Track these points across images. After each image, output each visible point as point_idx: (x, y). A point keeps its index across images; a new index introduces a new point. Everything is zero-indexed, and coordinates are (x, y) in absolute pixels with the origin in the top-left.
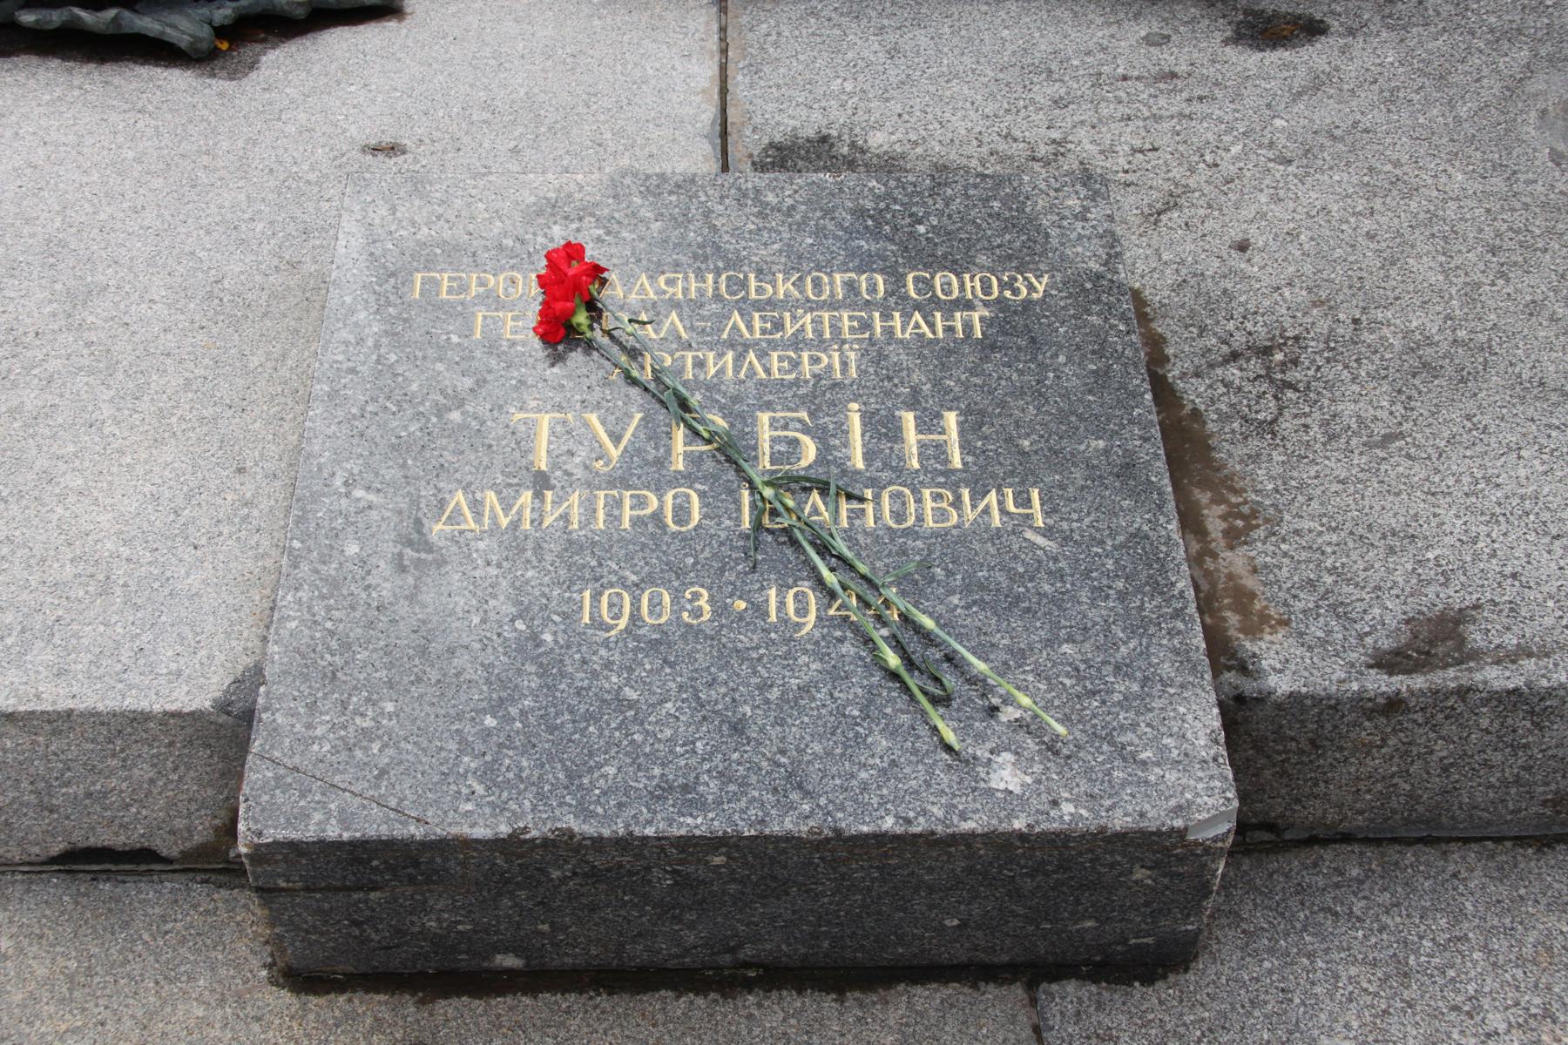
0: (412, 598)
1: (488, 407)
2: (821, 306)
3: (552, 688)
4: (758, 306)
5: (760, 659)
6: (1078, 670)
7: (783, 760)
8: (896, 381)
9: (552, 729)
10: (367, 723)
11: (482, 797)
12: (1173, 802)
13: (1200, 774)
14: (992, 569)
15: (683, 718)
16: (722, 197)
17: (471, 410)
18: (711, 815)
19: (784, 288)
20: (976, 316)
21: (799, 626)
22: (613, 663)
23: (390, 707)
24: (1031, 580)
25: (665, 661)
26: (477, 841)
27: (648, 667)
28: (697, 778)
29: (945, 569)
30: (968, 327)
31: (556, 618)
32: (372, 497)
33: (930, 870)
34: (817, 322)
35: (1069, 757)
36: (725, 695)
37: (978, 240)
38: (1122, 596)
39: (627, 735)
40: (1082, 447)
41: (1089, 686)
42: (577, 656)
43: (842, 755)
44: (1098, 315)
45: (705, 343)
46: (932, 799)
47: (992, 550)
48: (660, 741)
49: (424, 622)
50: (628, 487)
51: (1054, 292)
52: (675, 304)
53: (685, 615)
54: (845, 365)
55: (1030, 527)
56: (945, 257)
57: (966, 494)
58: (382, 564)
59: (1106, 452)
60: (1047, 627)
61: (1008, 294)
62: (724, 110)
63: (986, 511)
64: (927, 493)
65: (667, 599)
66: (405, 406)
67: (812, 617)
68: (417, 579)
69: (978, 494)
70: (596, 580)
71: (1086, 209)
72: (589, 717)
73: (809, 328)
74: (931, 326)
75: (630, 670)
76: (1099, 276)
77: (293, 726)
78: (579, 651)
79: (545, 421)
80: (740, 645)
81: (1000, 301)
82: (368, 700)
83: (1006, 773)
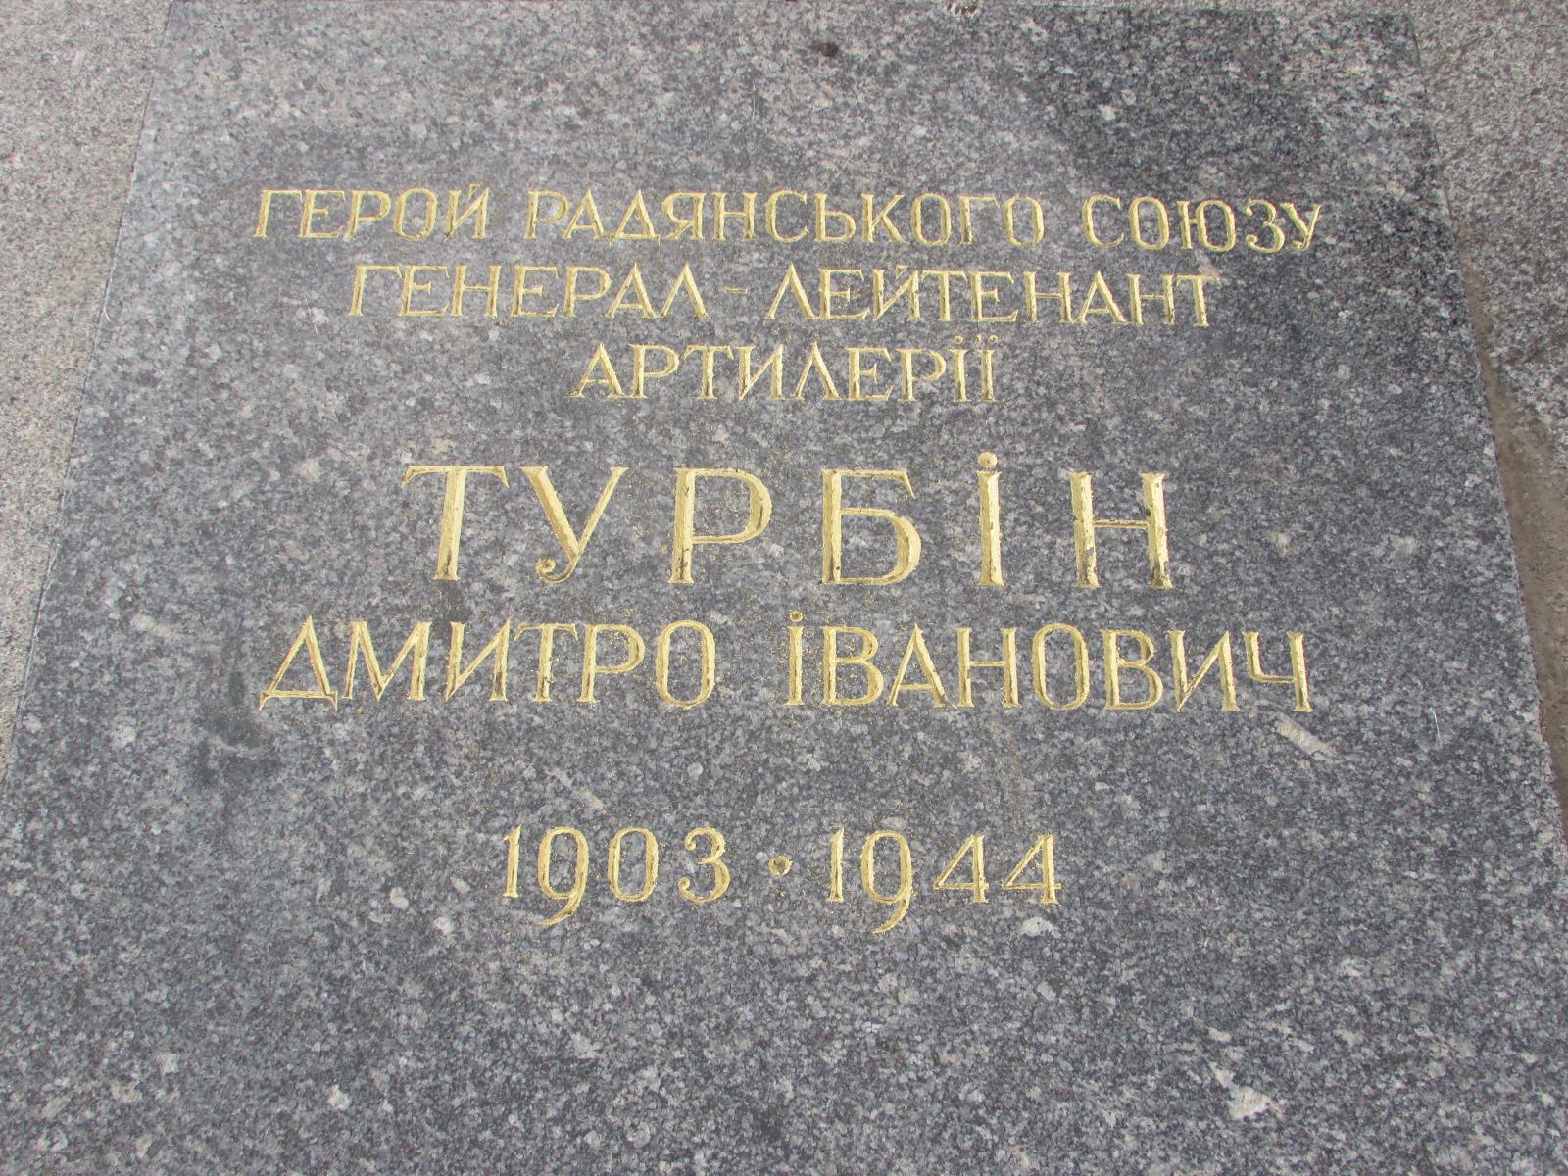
0: (219, 838)
1: (366, 451)
2: (936, 257)
3: (447, 1031)
4: (832, 256)
5: (811, 980)
6: (1365, 1011)
8: (1062, 409)
10: (131, 1097)
14: (1220, 798)
15: (672, 1101)
16: (777, 48)
19: (876, 221)
20: (1199, 282)
21: (881, 912)
22: (553, 982)
23: (169, 1063)
24: (1288, 823)
25: (647, 981)
29: (1140, 797)
30: (1185, 301)
31: (460, 885)
32: (165, 632)
34: (929, 288)
36: (748, 1055)
37: (1204, 136)
38: (1447, 857)
39: (574, 1134)
40: (1378, 551)
41: (1388, 1048)
42: (493, 966)
44: (1405, 288)
45: (738, 328)
47: (1222, 759)
48: (630, 1146)
49: (236, 888)
50: (595, 619)
51: (1330, 240)
52: (687, 252)
53: (685, 886)
54: (974, 373)
55: (1289, 712)
56: (1148, 162)
57: (1178, 639)
58: (172, 768)
59: (1420, 561)
60: (1315, 920)
61: (1253, 242)
63: (1213, 678)
64: (1111, 639)
65: (653, 850)
66: (230, 448)
67: (906, 893)
68: (228, 798)
70: (534, 806)
71: (1382, 83)
72: (513, 1096)
73: (916, 303)
74: (1123, 300)
75: (585, 996)
76: (1406, 212)
78: (496, 956)
79: (458, 479)
81: (1236, 255)
82: (135, 1046)
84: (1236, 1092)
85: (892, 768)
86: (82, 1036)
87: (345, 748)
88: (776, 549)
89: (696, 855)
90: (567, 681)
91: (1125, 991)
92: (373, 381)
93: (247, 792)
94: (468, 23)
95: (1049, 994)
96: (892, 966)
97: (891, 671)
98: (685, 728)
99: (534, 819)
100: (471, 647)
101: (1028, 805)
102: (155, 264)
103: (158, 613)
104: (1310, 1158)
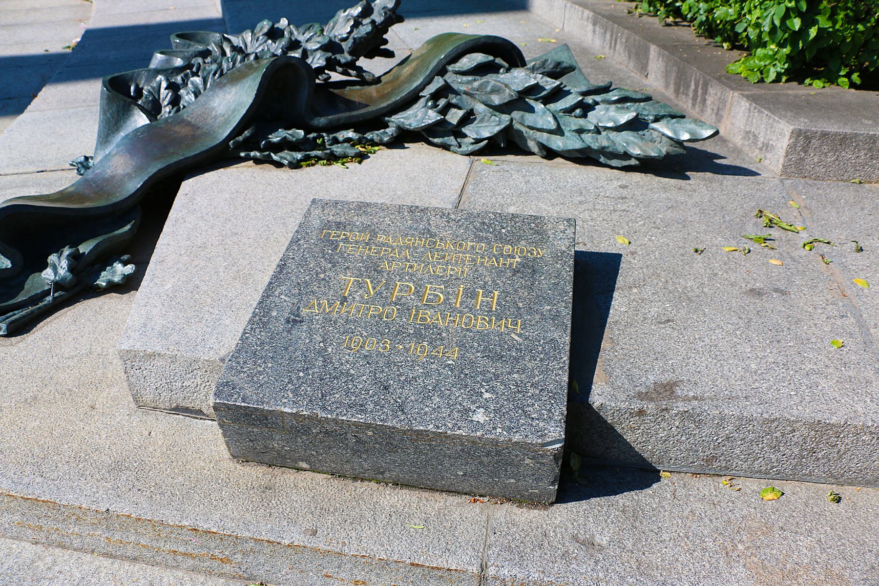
0: (289, 332)
10: (261, 369)
12: (540, 433)
23: (270, 365)
32: (286, 299)
33: (448, 449)
38: (541, 360)
52: (408, 247)
59: (550, 311)
62: (460, 196)
76: (564, 252)
103: (286, 295)
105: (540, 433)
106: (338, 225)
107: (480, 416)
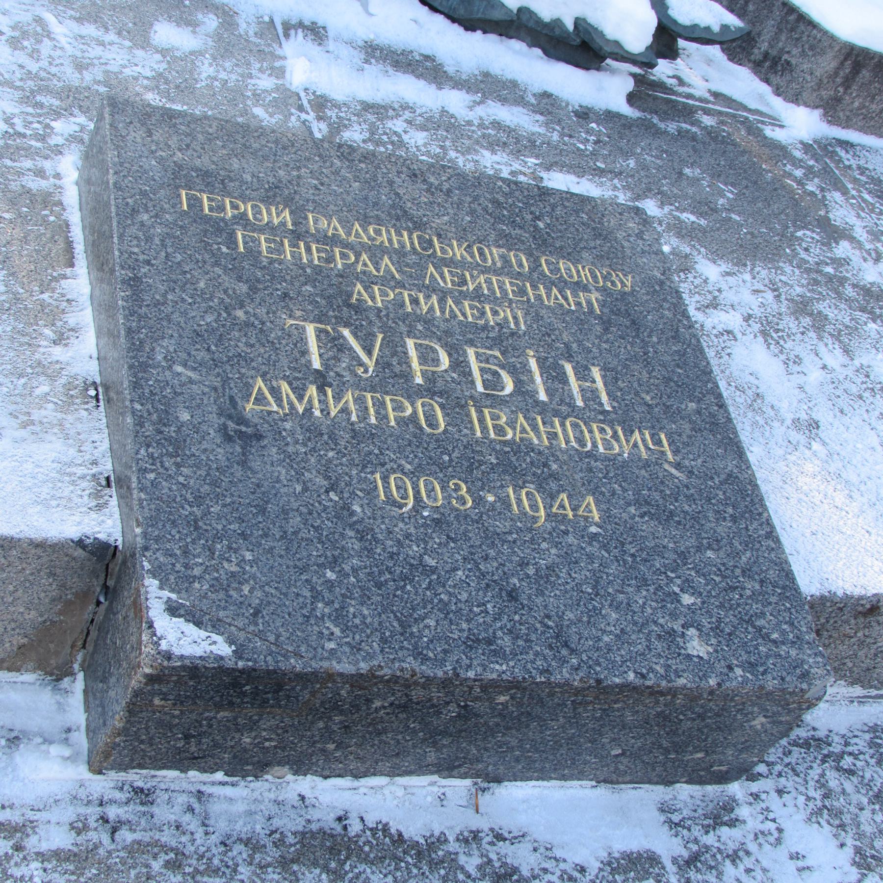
0: (243, 463)
5: (514, 542)
6: (719, 570)
7: (550, 623)
9: (379, 585)
10: (234, 568)
11: (340, 638)
13: (809, 652)
17: (251, 310)
18: (511, 663)
19: (458, 252)
21: (535, 519)
22: (410, 535)
24: (676, 501)
25: (448, 536)
26: (341, 675)
27: (437, 540)
28: (494, 633)
30: (589, 303)
31: (359, 493)
35: (730, 634)
36: (497, 569)
39: (436, 595)
42: (383, 527)
43: (589, 622)
44: (669, 309)
46: (654, 660)
48: (460, 601)
49: (258, 486)
52: (383, 250)
56: (561, 248)
58: (211, 431)
59: (699, 412)
61: (609, 284)
63: (635, 445)
69: (628, 432)
72: (405, 578)
74: (566, 299)
75: (426, 543)
77: (173, 565)
78: (383, 523)
80: (498, 530)
82: (230, 548)
83: (695, 643)
84: (681, 594)
85: (524, 466)
86: (202, 542)
87: (292, 433)
88: (455, 375)
89: (456, 490)
90: (382, 417)
91: (633, 555)
92: (258, 281)
93: (251, 446)
94: (256, 134)
95: (606, 555)
96: (545, 540)
97: (514, 429)
98: (437, 441)
99: (383, 470)
100: (337, 398)
101: (579, 484)
102: (134, 211)
103: (185, 365)
104: (714, 620)
105: (798, 671)
106: (209, 180)
107: (697, 647)
